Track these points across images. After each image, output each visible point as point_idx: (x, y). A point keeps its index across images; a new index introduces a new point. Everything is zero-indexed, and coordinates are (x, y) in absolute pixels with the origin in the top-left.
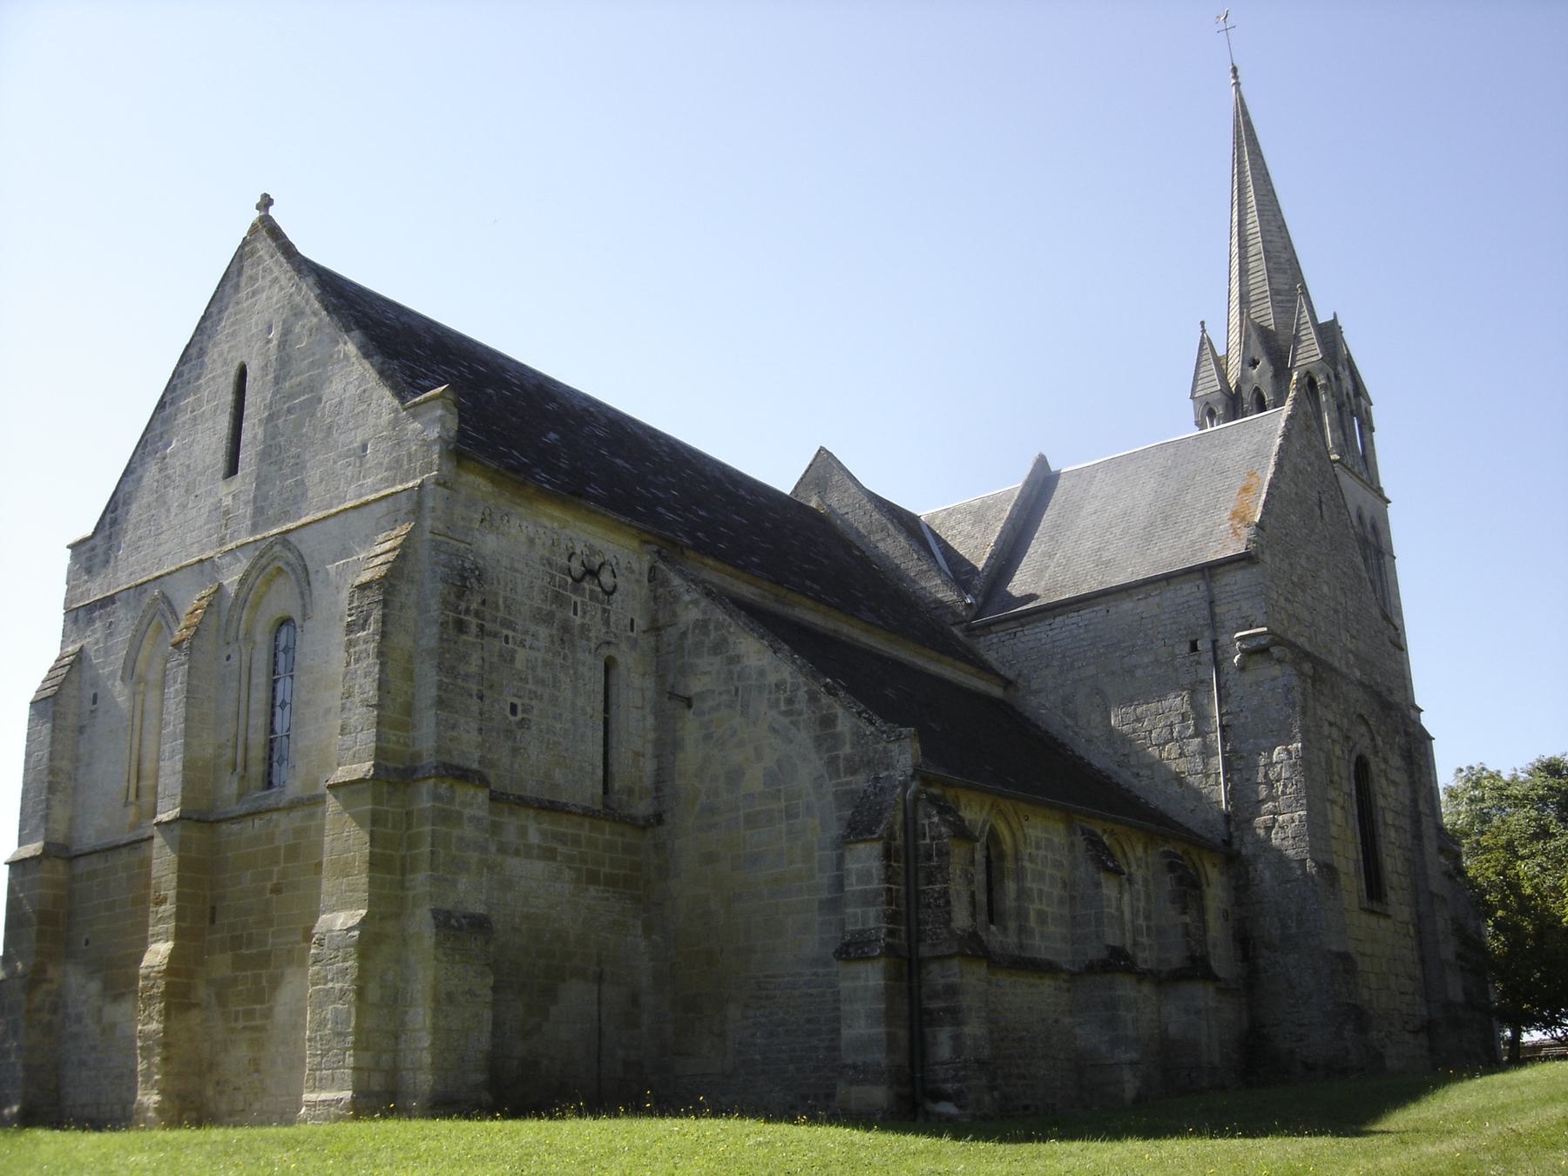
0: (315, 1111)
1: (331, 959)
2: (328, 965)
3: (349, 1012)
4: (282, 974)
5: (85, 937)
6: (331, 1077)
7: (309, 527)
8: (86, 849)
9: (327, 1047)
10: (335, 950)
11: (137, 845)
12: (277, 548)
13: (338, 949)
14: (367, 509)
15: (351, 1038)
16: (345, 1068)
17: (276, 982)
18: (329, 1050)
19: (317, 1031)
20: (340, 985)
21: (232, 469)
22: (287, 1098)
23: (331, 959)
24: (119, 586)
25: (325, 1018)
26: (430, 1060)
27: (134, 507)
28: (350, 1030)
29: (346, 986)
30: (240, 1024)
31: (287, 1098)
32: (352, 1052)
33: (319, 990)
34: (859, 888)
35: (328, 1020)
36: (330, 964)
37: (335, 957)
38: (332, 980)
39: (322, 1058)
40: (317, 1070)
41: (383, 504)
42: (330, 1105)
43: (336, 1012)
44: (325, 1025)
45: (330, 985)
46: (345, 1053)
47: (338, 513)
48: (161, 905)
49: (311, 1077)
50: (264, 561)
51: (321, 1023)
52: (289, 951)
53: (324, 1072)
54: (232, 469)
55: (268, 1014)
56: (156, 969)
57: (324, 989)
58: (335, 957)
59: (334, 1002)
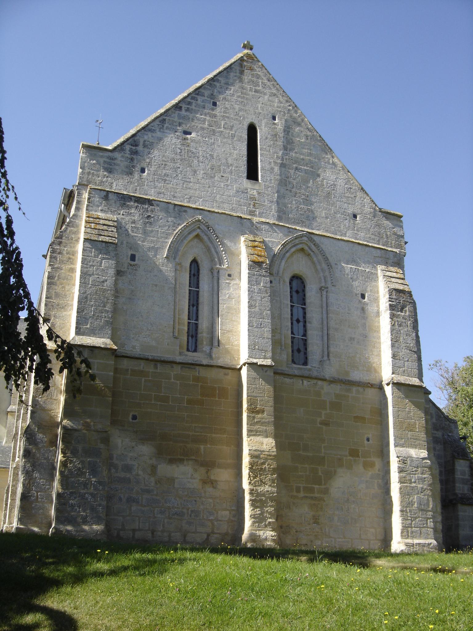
0: (413, 549)
1: (413, 471)
2: (411, 474)
3: (428, 500)
4: (335, 472)
5: (366, 436)
6: (419, 532)
7: (327, 238)
8: (129, 354)
9: (415, 516)
10: (415, 467)
11: (192, 366)
12: (305, 238)
13: (417, 467)
14: (367, 248)
15: (430, 513)
16: (428, 528)
17: (330, 475)
18: (416, 518)
19: (407, 507)
20: (421, 486)
21: (252, 174)
22: (343, 540)
23: (413, 471)
24: (147, 195)
25: (412, 501)
26: (441, 528)
27: (156, 153)
28: (430, 509)
29: (425, 487)
30: (302, 494)
31: (343, 540)
32: (431, 520)
33: (407, 486)
34: (461, 477)
35: (415, 502)
36: (413, 474)
37: (416, 471)
38: (415, 482)
39: (412, 521)
40: (408, 527)
41: (378, 251)
42: (424, 546)
43: (420, 499)
44: (412, 505)
45: (414, 485)
46: (427, 521)
47: (348, 241)
48: (258, 414)
49: (405, 530)
50: (297, 241)
51: (409, 503)
52: (340, 459)
53: (414, 529)
54: (252, 174)
55: (326, 491)
56: (267, 453)
57: (410, 487)
58: (416, 471)
59: (418, 494)
